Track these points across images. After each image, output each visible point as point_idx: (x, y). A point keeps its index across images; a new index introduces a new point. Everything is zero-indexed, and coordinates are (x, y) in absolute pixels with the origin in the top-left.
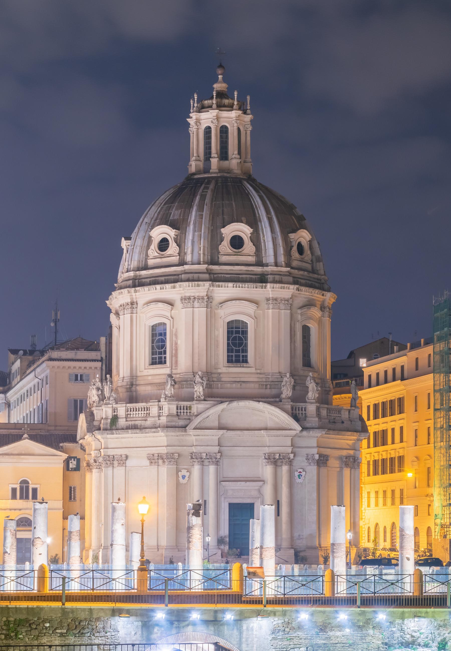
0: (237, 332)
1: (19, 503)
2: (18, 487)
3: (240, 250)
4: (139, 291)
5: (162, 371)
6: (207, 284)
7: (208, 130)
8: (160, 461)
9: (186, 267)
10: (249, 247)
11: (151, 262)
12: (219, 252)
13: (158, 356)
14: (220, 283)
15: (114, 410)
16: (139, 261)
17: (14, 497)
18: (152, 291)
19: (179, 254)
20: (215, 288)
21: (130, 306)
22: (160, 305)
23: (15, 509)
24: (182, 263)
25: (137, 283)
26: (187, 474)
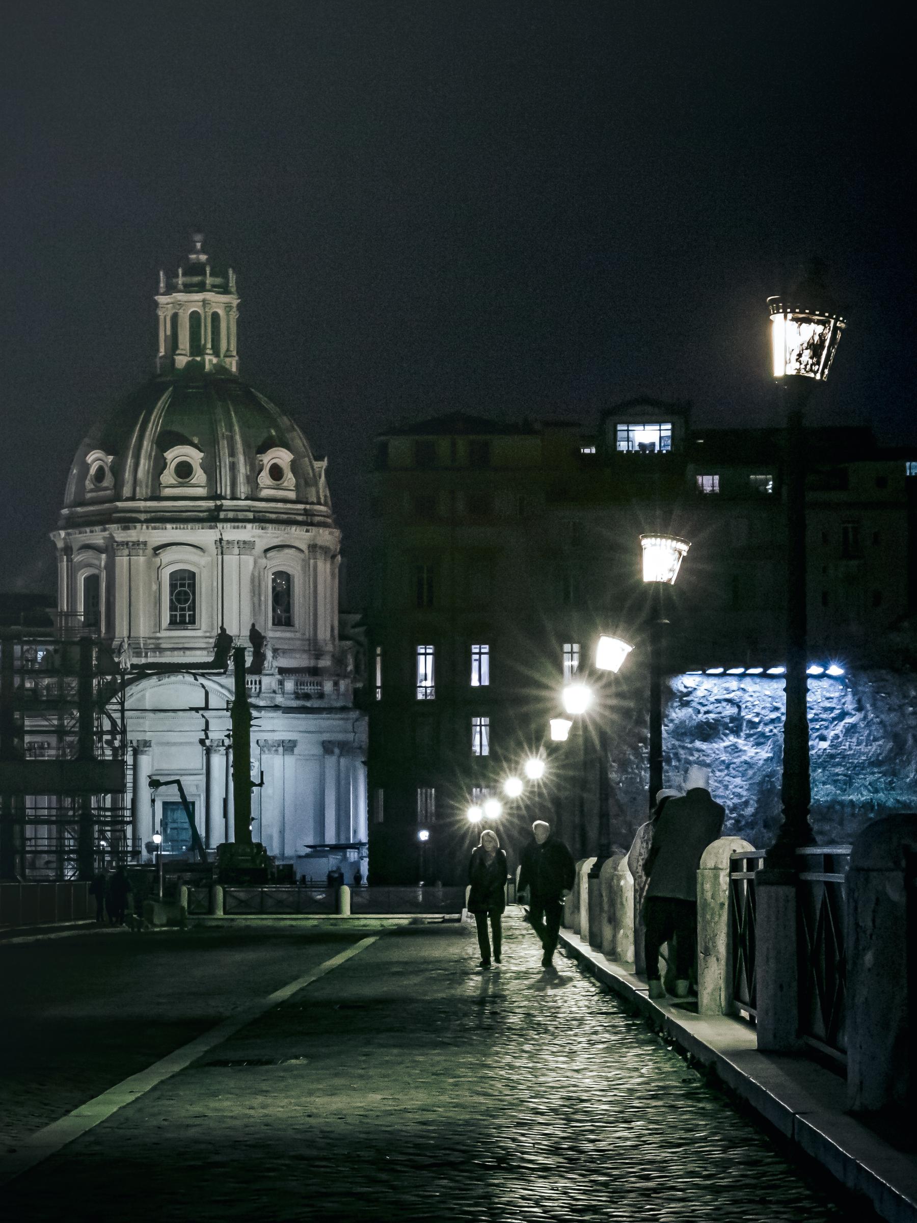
3: (187, 480)
9: (119, 504)
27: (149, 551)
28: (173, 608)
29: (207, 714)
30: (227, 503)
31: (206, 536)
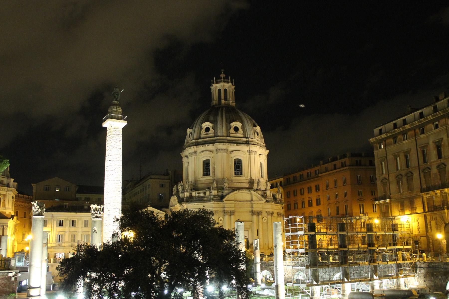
0: (238, 163)
5: (208, 179)
6: (227, 144)
7: (219, 90)
9: (218, 137)
10: (241, 131)
11: (202, 136)
19: (214, 133)
22: (207, 152)
24: (216, 136)
25: (197, 144)
26: (222, 219)
27: (229, 152)
28: (235, 170)
29: (252, 202)
30: (250, 139)
31: (245, 148)
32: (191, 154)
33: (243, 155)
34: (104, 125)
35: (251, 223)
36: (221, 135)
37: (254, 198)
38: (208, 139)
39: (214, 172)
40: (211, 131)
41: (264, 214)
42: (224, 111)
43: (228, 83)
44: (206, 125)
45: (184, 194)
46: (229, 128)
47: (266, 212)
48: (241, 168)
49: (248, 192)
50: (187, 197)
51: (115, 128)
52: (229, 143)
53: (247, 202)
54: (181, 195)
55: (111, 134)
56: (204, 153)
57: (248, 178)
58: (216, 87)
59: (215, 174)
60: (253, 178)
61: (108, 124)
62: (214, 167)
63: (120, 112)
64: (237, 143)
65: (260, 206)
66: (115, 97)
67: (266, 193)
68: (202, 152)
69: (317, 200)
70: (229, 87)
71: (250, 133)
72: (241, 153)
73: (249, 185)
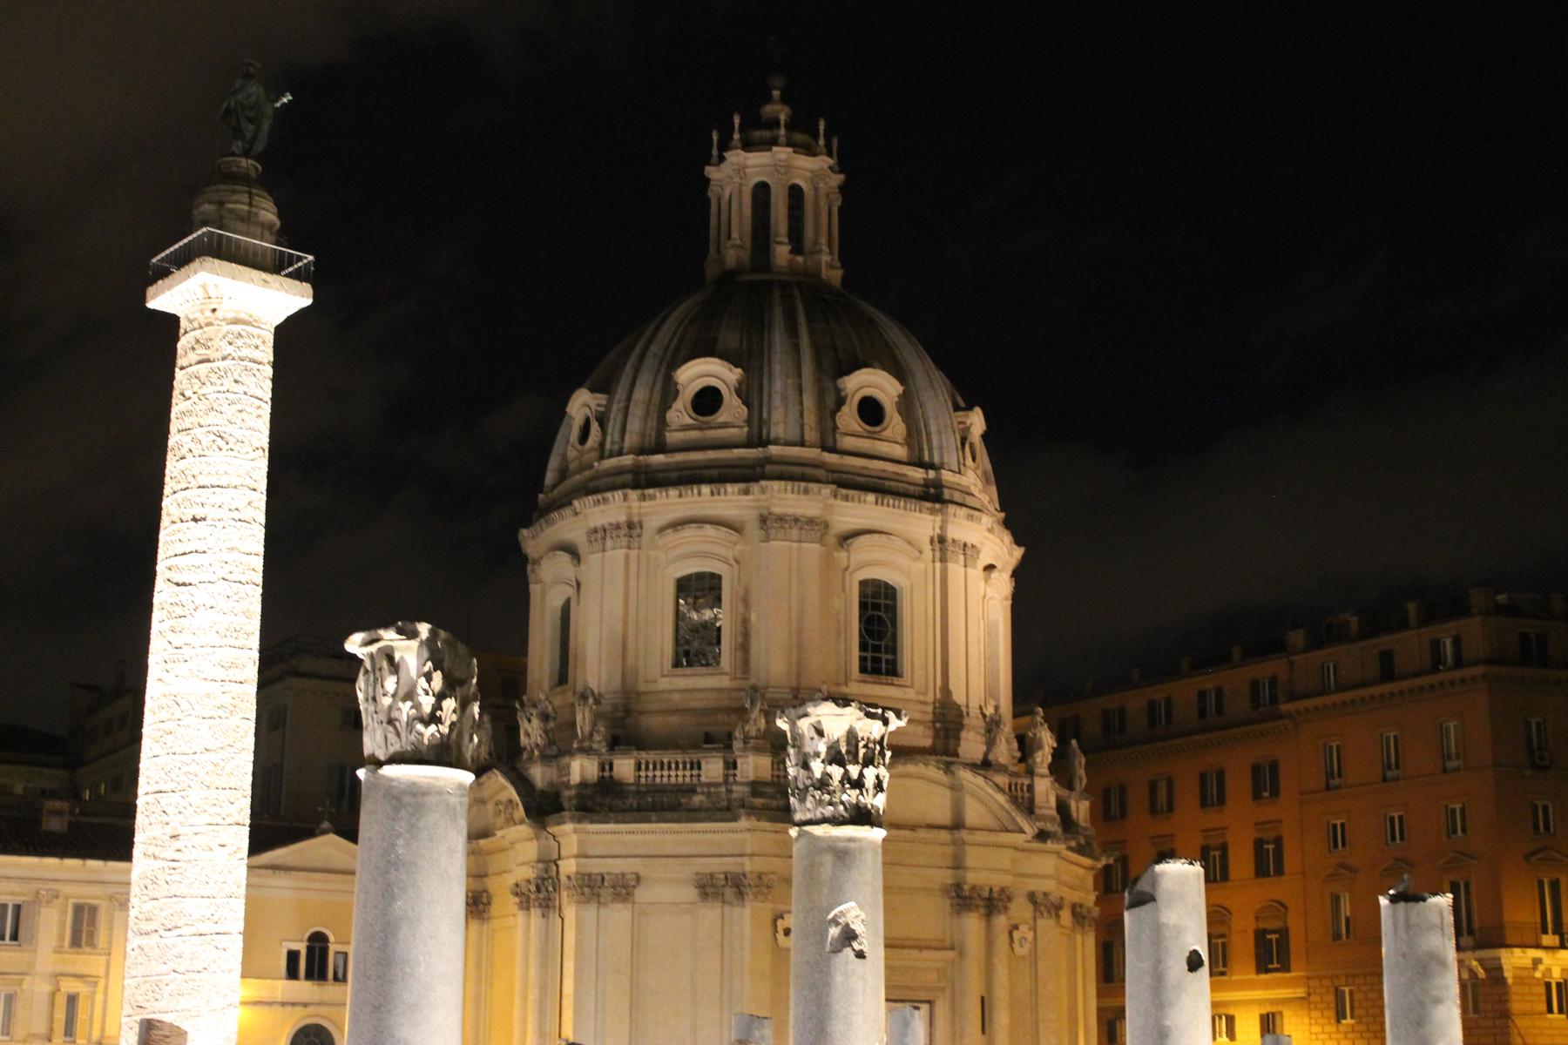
0: (876, 607)
1: (304, 988)
2: (302, 947)
4: (653, 498)
6: (827, 490)
8: (729, 892)
9: (774, 450)
10: (895, 424)
12: (835, 428)
13: (694, 647)
14: (851, 493)
15: (606, 766)
16: (643, 435)
17: (292, 973)
18: (690, 499)
19: (749, 422)
20: (839, 502)
21: (625, 530)
22: (709, 530)
23: (294, 1004)
25: (645, 480)
27: (831, 539)
28: (863, 646)
29: (964, 834)
30: (947, 476)
31: (920, 523)
32: (600, 534)
33: (905, 562)
34: (162, 299)
35: (951, 954)
36: (793, 434)
37: (974, 813)
38: (711, 455)
39: (744, 647)
40: (733, 409)
41: (1020, 909)
42: (800, 309)
43: (811, 152)
44: (698, 373)
45: (566, 770)
46: (830, 401)
47: (1032, 897)
48: (894, 636)
49: (940, 775)
50: (583, 785)
51: (236, 322)
52: (843, 484)
53: (933, 834)
54: (539, 774)
55: (211, 354)
56: (688, 532)
57: (930, 698)
58: (741, 170)
59: (746, 662)
60: (959, 697)
61: (186, 294)
62: (745, 621)
63: (270, 226)
64: (881, 488)
65: (1005, 859)
66: (238, 133)
67: (1031, 788)
68: (677, 525)
69: (1259, 844)
70: (815, 177)
71: (943, 445)
72: (895, 543)
73: (936, 737)
